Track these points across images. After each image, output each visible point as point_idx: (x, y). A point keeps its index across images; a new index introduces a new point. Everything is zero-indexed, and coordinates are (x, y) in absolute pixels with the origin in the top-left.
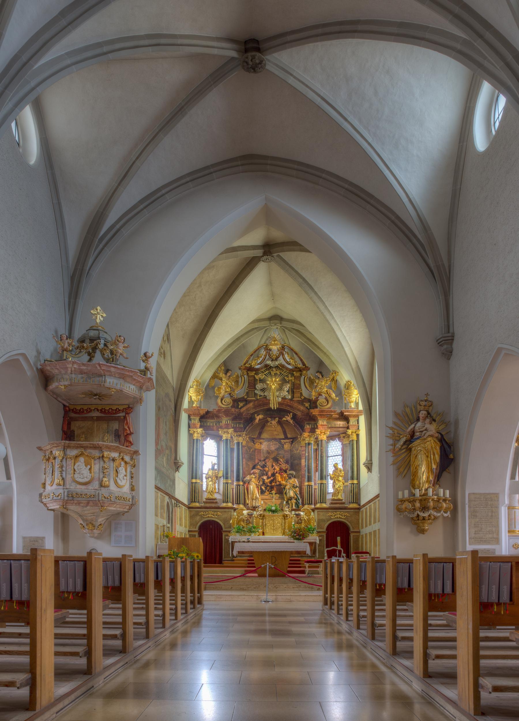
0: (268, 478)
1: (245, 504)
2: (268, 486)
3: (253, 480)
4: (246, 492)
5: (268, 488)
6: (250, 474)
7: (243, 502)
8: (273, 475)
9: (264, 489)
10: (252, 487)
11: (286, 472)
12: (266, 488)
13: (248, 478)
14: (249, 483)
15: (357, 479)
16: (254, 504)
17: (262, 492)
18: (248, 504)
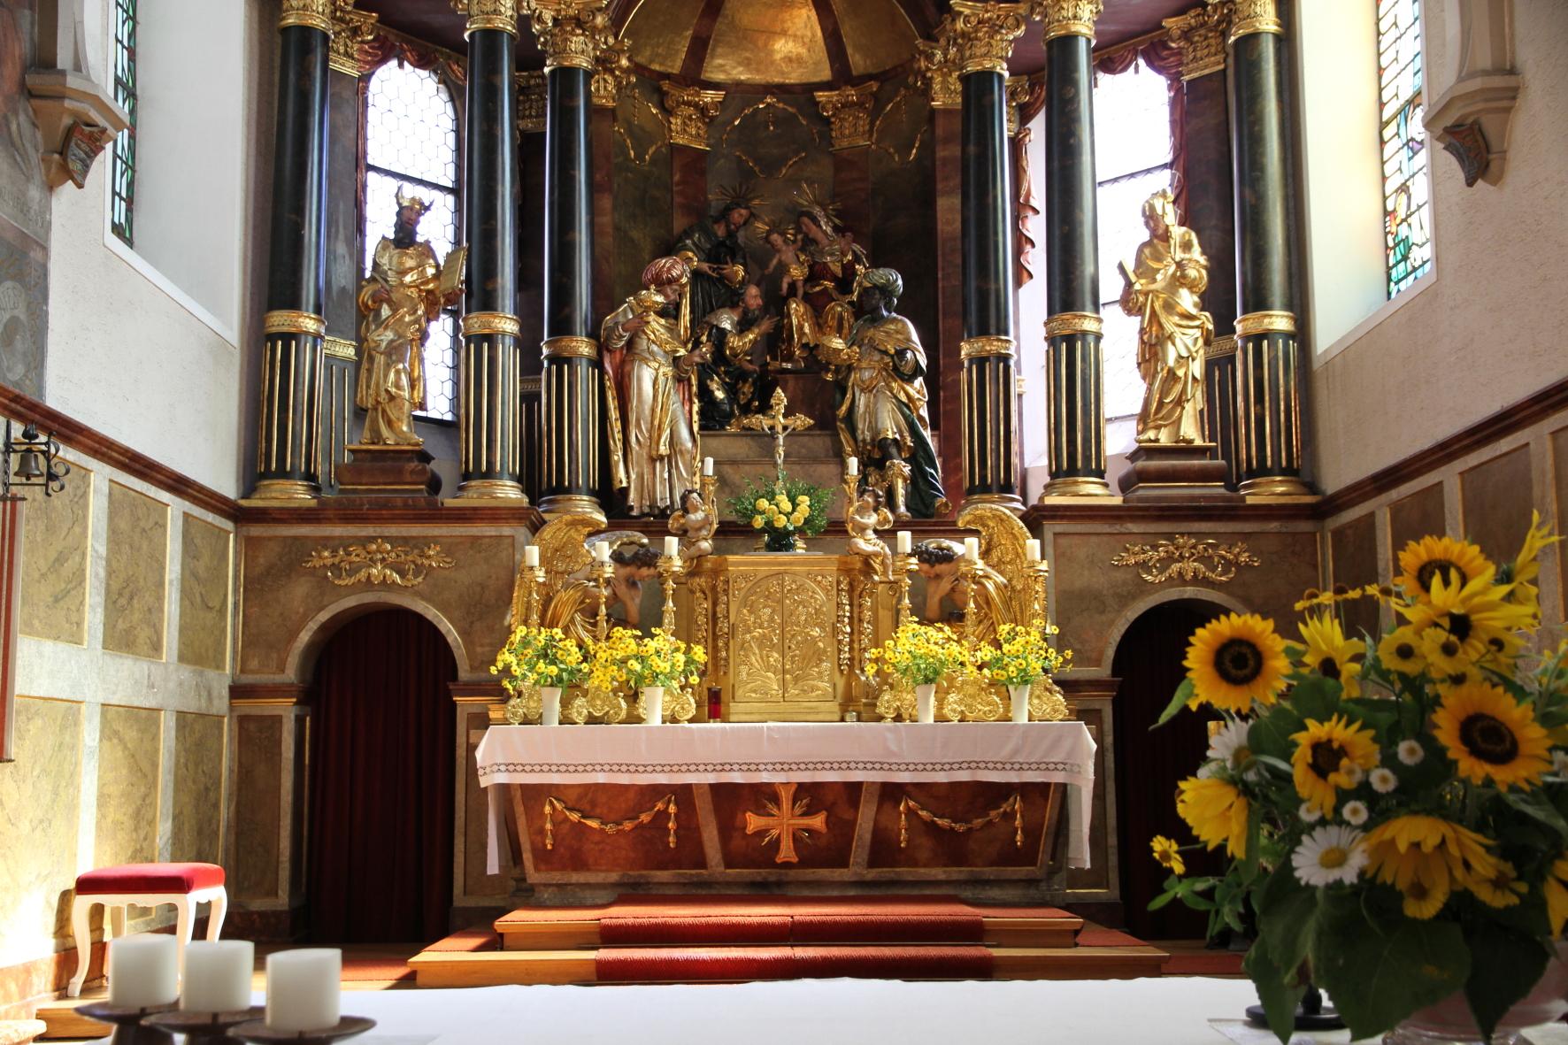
0: (743, 326)
1: (610, 498)
2: (742, 375)
3: (657, 325)
4: (612, 404)
5: (747, 389)
6: (636, 286)
7: (595, 480)
8: (776, 303)
9: (720, 395)
10: (649, 378)
11: (844, 284)
12: (731, 390)
13: (625, 312)
14: (630, 344)
15: (1289, 306)
16: (662, 496)
17: (712, 419)
18: (625, 491)
